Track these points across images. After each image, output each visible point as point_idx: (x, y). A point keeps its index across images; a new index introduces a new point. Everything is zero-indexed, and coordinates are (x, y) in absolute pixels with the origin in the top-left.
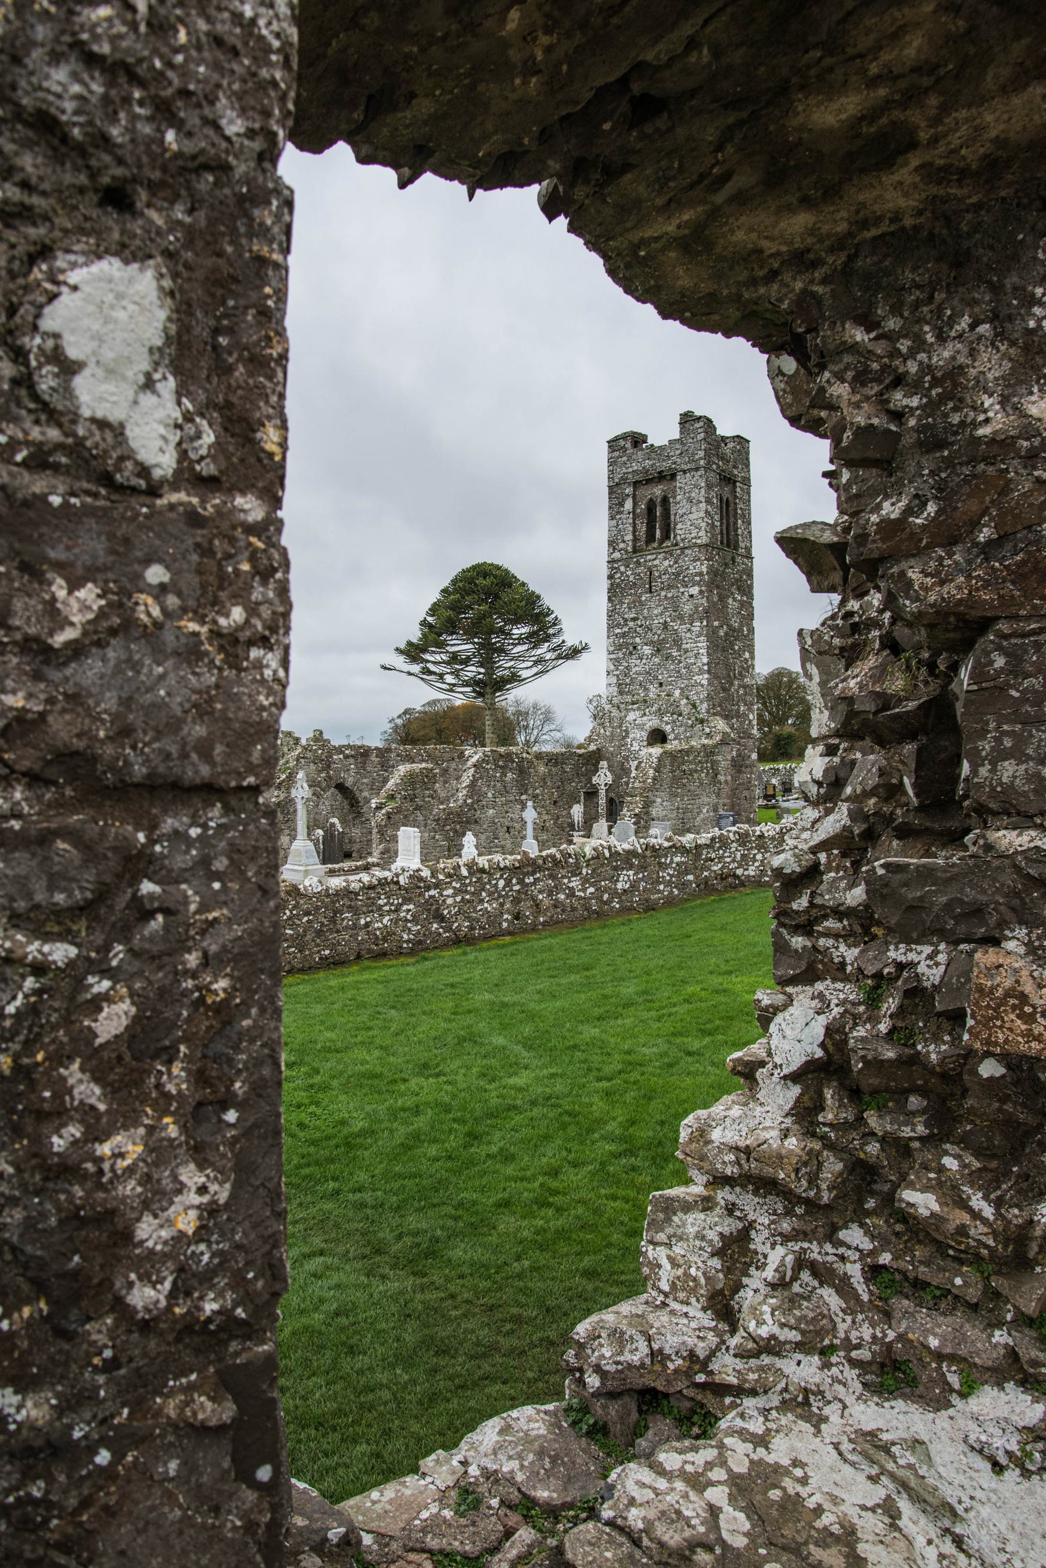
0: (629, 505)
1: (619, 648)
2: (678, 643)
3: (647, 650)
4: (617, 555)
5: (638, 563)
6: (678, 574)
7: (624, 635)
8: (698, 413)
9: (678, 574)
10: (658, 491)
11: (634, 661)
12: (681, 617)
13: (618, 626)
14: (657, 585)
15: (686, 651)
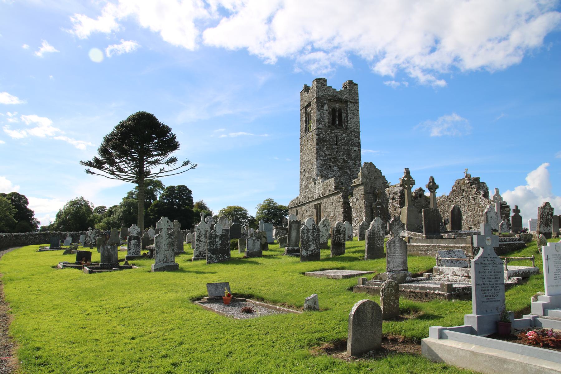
0: (326, 107)
1: (323, 165)
2: (349, 168)
3: (336, 168)
4: (321, 126)
5: (331, 133)
6: (349, 141)
7: (325, 160)
8: (355, 82)
9: (349, 141)
10: (337, 106)
11: (329, 172)
12: (351, 158)
13: (322, 156)
14: (340, 143)
15: (353, 171)
